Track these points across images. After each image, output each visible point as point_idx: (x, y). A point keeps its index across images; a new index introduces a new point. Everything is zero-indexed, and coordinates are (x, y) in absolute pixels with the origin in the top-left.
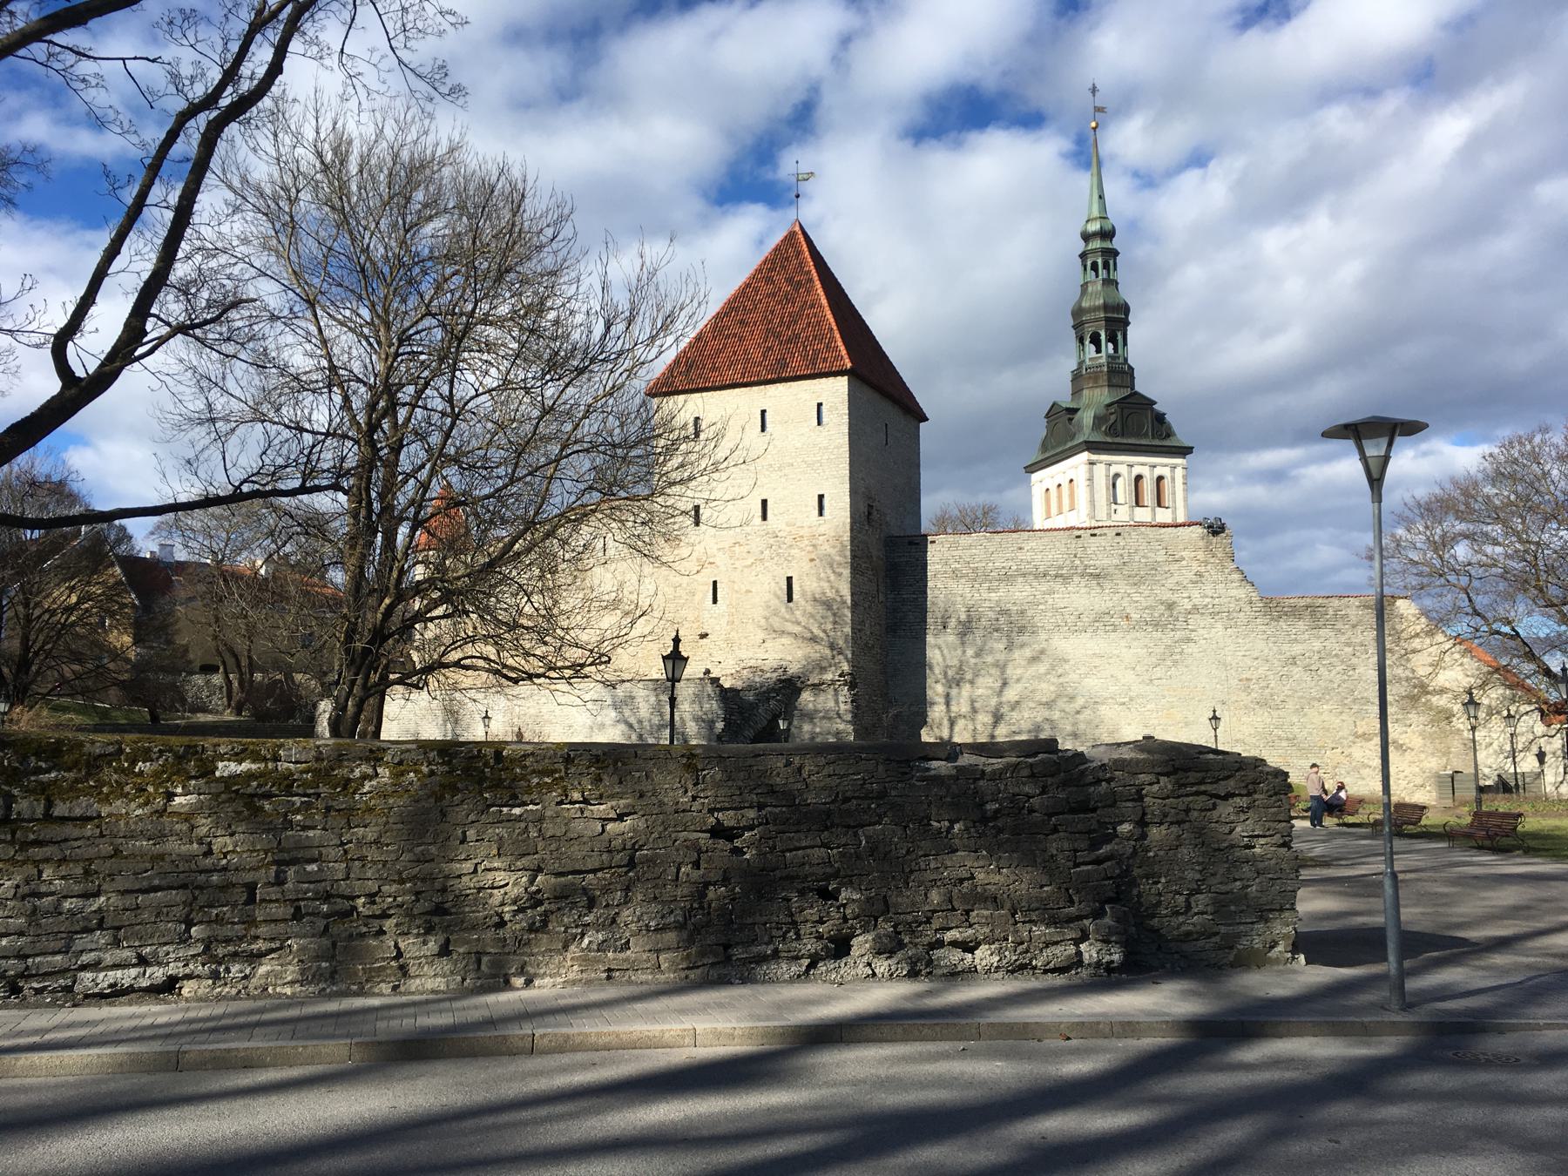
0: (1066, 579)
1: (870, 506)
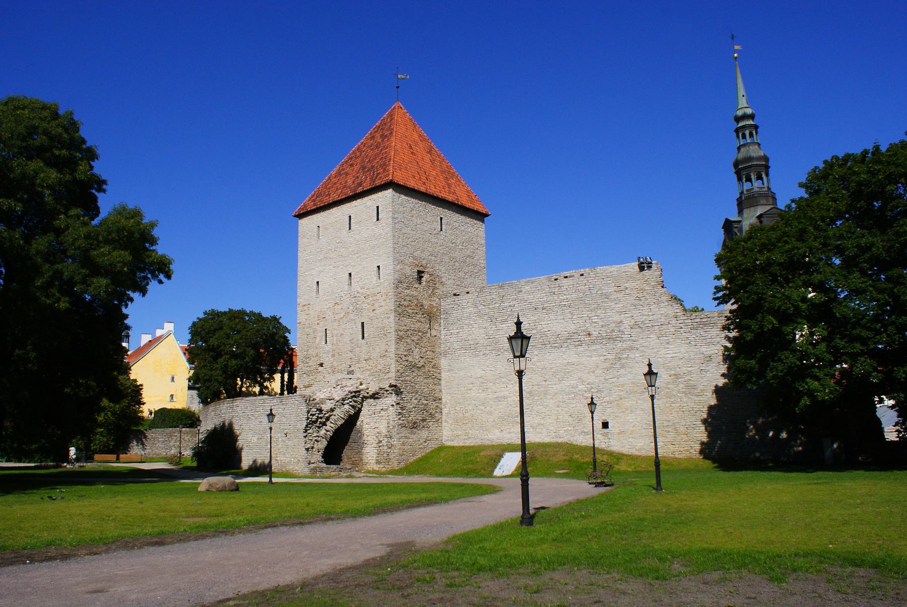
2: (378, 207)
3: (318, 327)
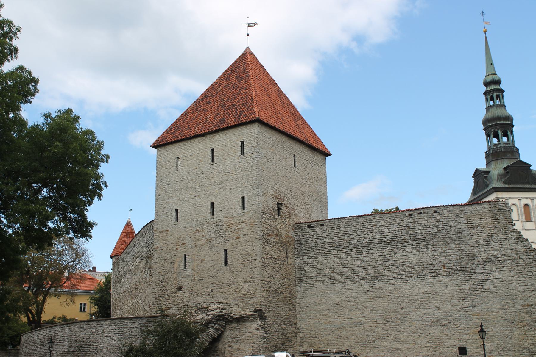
1: (278, 204)
2: (242, 143)
3: (176, 253)
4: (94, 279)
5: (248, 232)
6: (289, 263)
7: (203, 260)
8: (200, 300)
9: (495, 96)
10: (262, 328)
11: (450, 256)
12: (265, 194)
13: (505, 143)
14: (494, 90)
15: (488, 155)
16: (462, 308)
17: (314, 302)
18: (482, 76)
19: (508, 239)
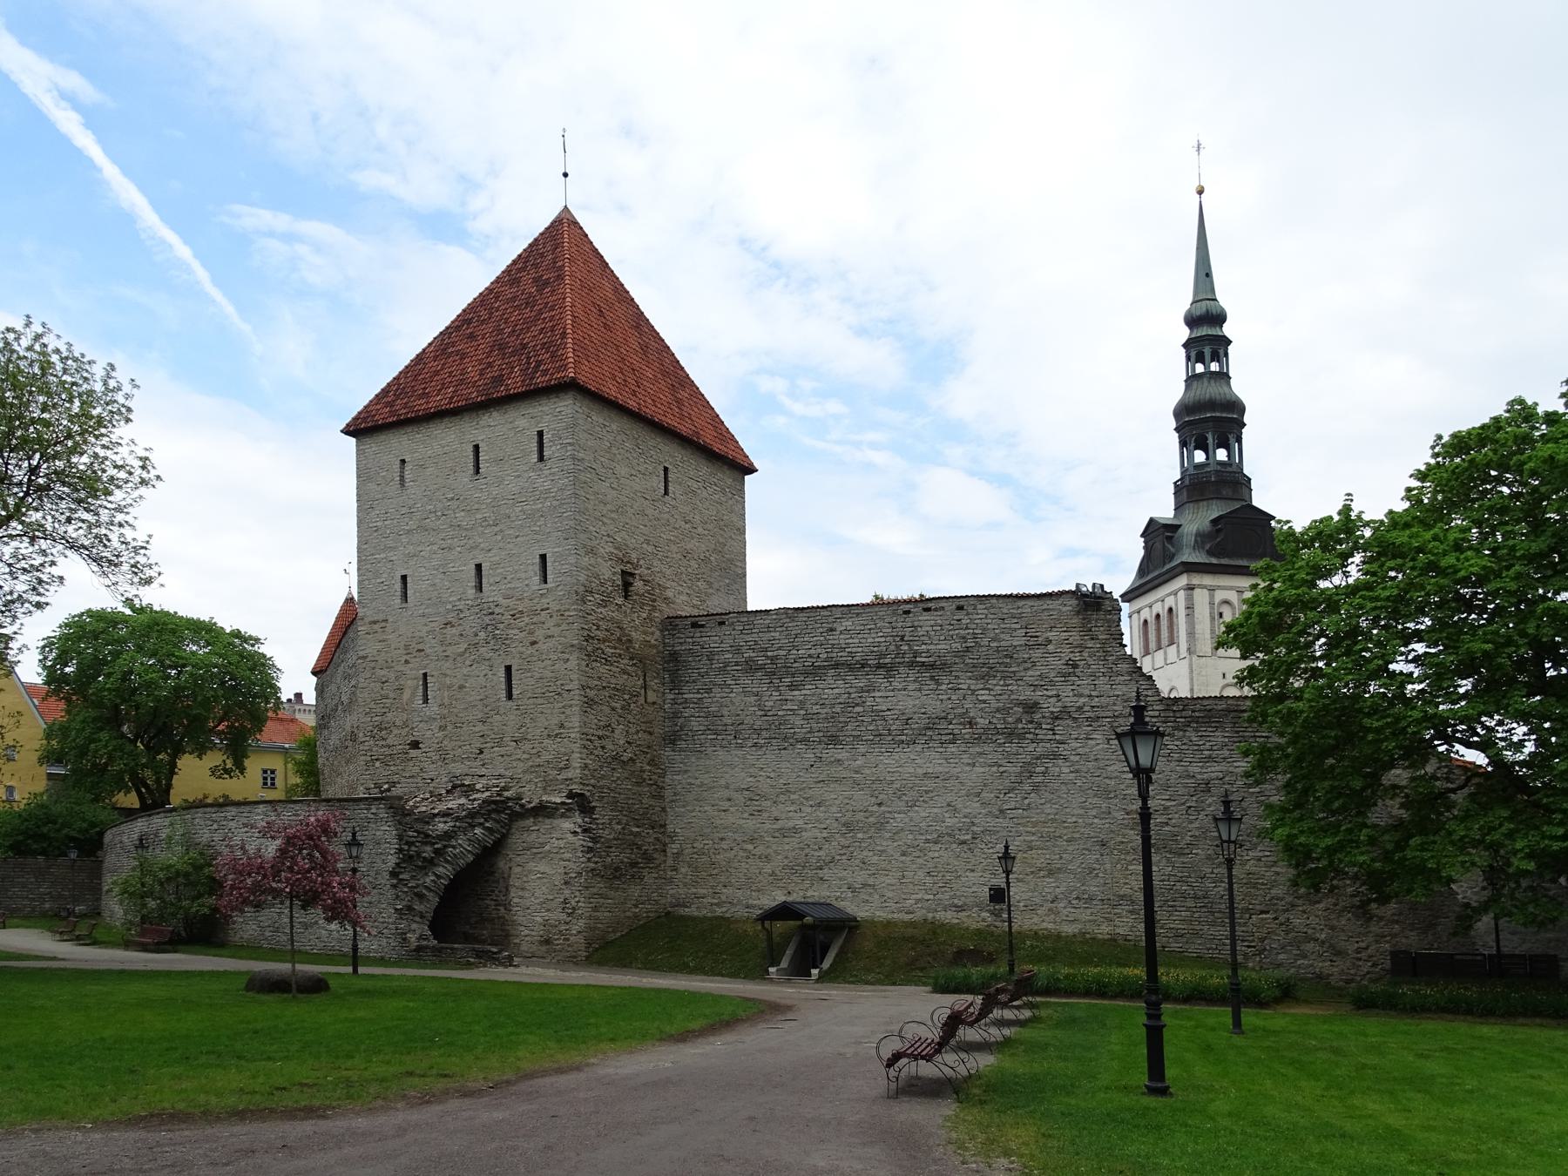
0: (889, 670)
2: (540, 434)
4: (293, 720)
5: (555, 631)
6: (650, 700)
7: (461, 687)
8: (458, 769)
9: (1207, 351)
10: (585, 831)
11: (984, 702)
12: (592, 551)
13: (1221, 463)
14: (1207, 334)
15: (1179, 489)
16: (1002, 811)
17: (702, 784)
18: (1183, 298)
19: (1111, 674)
